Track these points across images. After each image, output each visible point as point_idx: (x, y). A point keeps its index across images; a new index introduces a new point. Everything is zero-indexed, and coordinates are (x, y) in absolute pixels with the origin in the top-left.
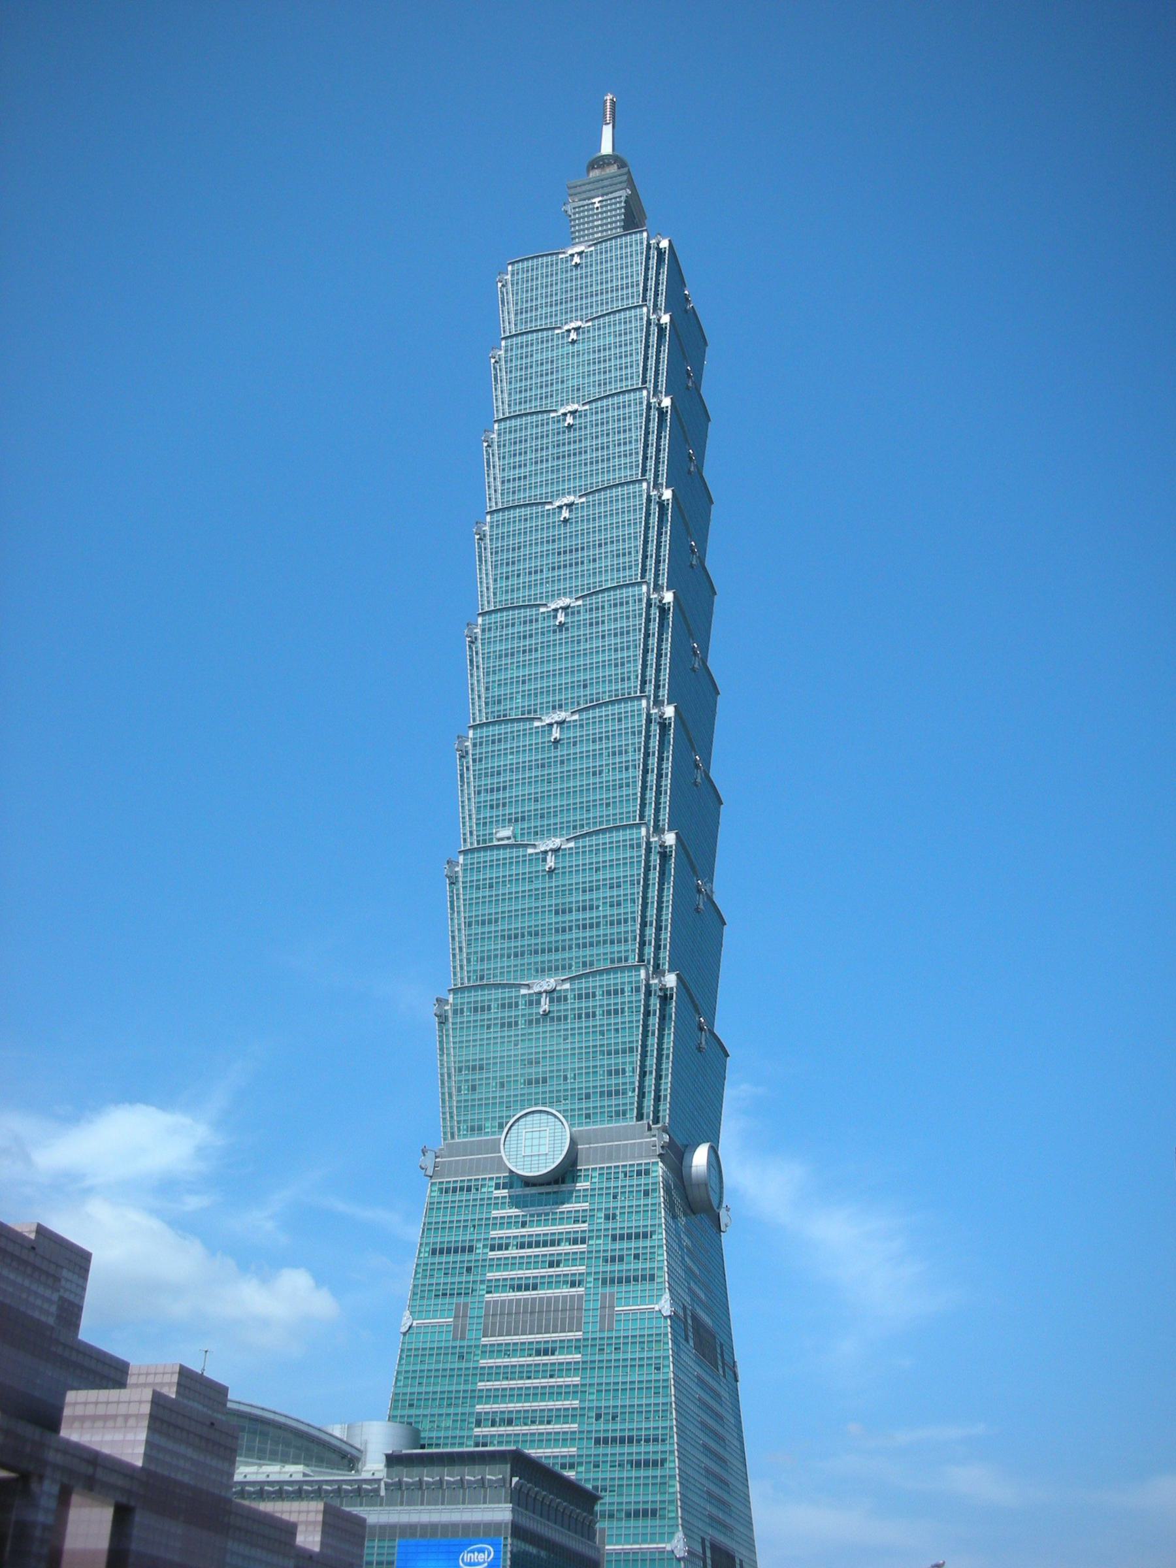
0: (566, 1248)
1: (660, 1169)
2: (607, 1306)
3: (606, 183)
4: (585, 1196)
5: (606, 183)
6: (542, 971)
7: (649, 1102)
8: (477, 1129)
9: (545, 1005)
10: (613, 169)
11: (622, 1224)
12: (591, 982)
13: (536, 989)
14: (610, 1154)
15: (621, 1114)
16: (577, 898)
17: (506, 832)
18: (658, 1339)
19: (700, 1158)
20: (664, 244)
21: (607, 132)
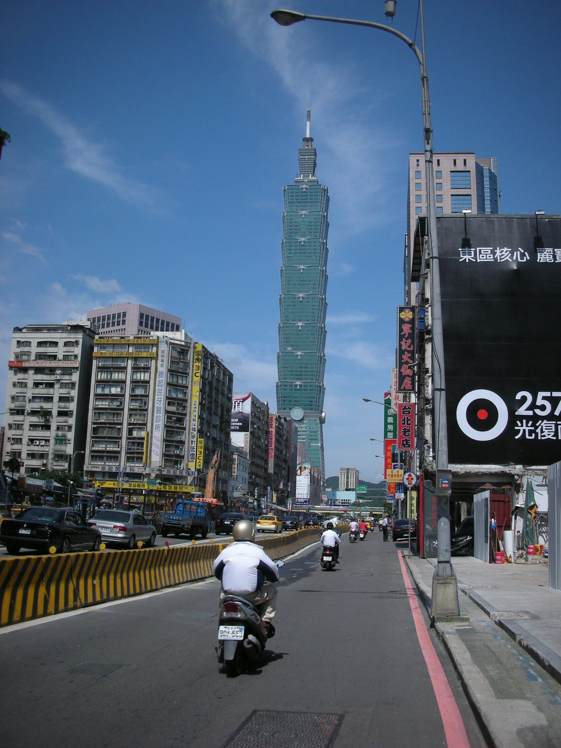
0: (302, 433)
1: (318, 421)
2: (310, 443)
3: (309, 151)
4: (305, 424)
5: (309, 151)
6: (297, 379)
7: (317, 407)
8: (285, 409)
9: (298, 388)
10: (310, 143)
11: (312, 430)
12: (307, 384)
13: (297, 383)
14: (310, 416)
15: (312, 409)
16: (304, 365)
17: (290, 349)
18: (318, 450)
19: (323, 414)
20: (326, 188)
21: (308, 123)
